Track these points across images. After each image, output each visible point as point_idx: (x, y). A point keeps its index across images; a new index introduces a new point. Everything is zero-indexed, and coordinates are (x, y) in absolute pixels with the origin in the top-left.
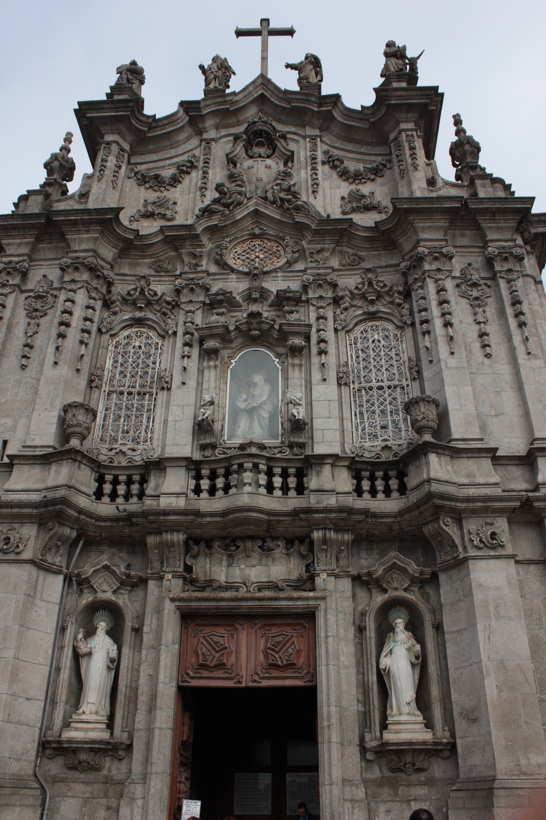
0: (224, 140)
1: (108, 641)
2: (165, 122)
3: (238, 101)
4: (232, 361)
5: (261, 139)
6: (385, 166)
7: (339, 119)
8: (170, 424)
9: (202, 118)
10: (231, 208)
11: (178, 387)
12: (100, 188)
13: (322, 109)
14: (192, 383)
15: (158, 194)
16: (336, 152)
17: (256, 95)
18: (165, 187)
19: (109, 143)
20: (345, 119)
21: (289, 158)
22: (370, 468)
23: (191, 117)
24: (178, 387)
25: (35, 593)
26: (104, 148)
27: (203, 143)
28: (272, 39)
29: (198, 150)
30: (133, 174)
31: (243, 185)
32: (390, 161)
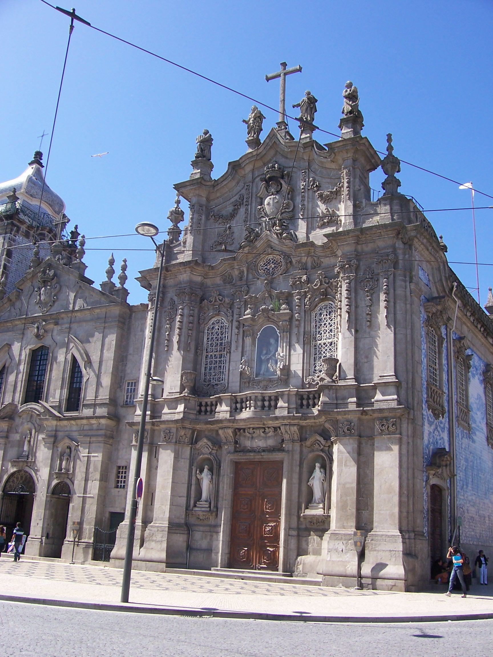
1: (209, 473)
2: (222, 180)
3: (261, 153)
4: (259, 334)
8: (231, 372)
11: (234, 351)
14: (240, 349)
22: (307, 393)
24: (234, 351)
25: (178, 456)
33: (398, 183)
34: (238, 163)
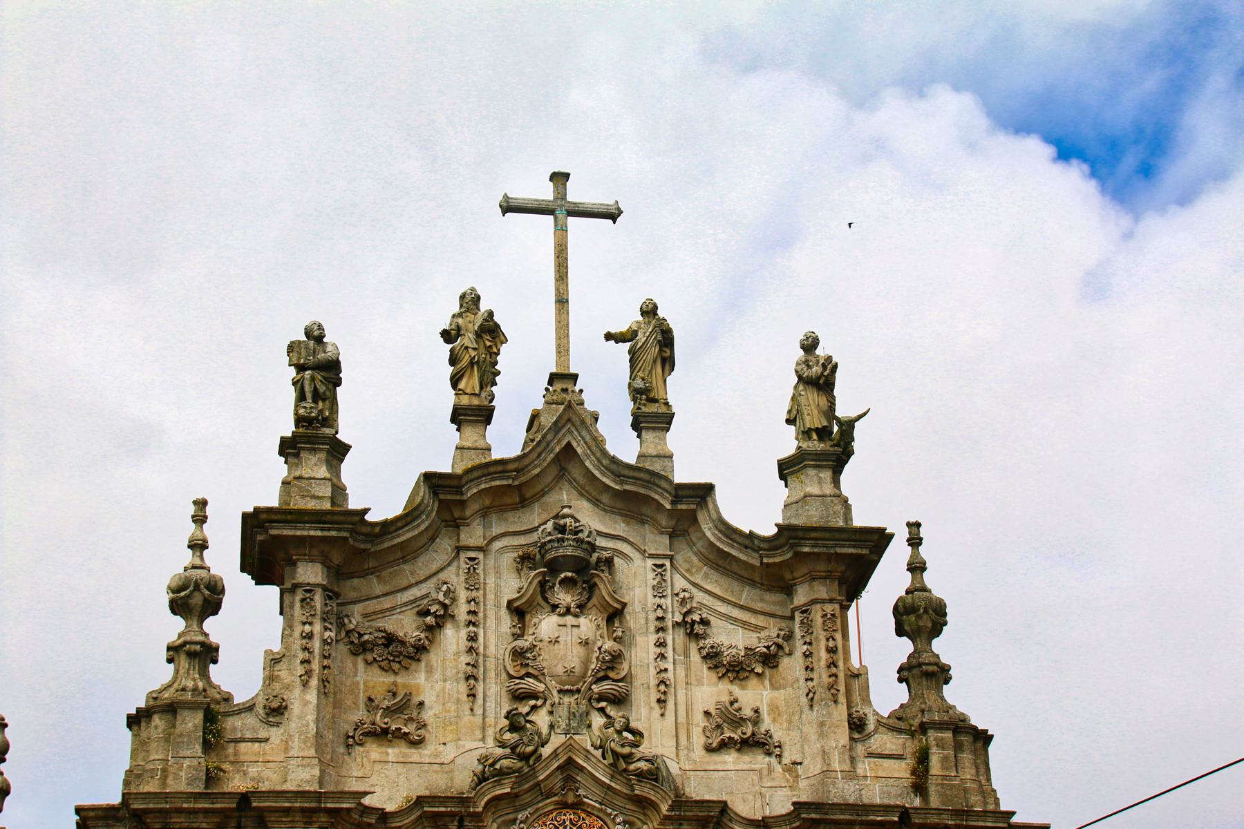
0: (497, 545)
5: (571, 572)
6: (780, 647)
7: (708, 534)
9: (462, 504)
10: (531, 762)
12: (306, 703)
13: (680, 507)
15: (389, 679)
16: (699, 596)
17: (557, 450)
18: (399, 662)
19: (310, 589)
20: (719, 539)
21: (615, 614)
23: (441, 501)
26: (303, 600)
27: (463, 556)
28: (575, 224)
29: (453, 568)
30: (343, 634)
31: (541, 678)
32: (789, 637)
33: (941, 674)
34: (455, 482)
